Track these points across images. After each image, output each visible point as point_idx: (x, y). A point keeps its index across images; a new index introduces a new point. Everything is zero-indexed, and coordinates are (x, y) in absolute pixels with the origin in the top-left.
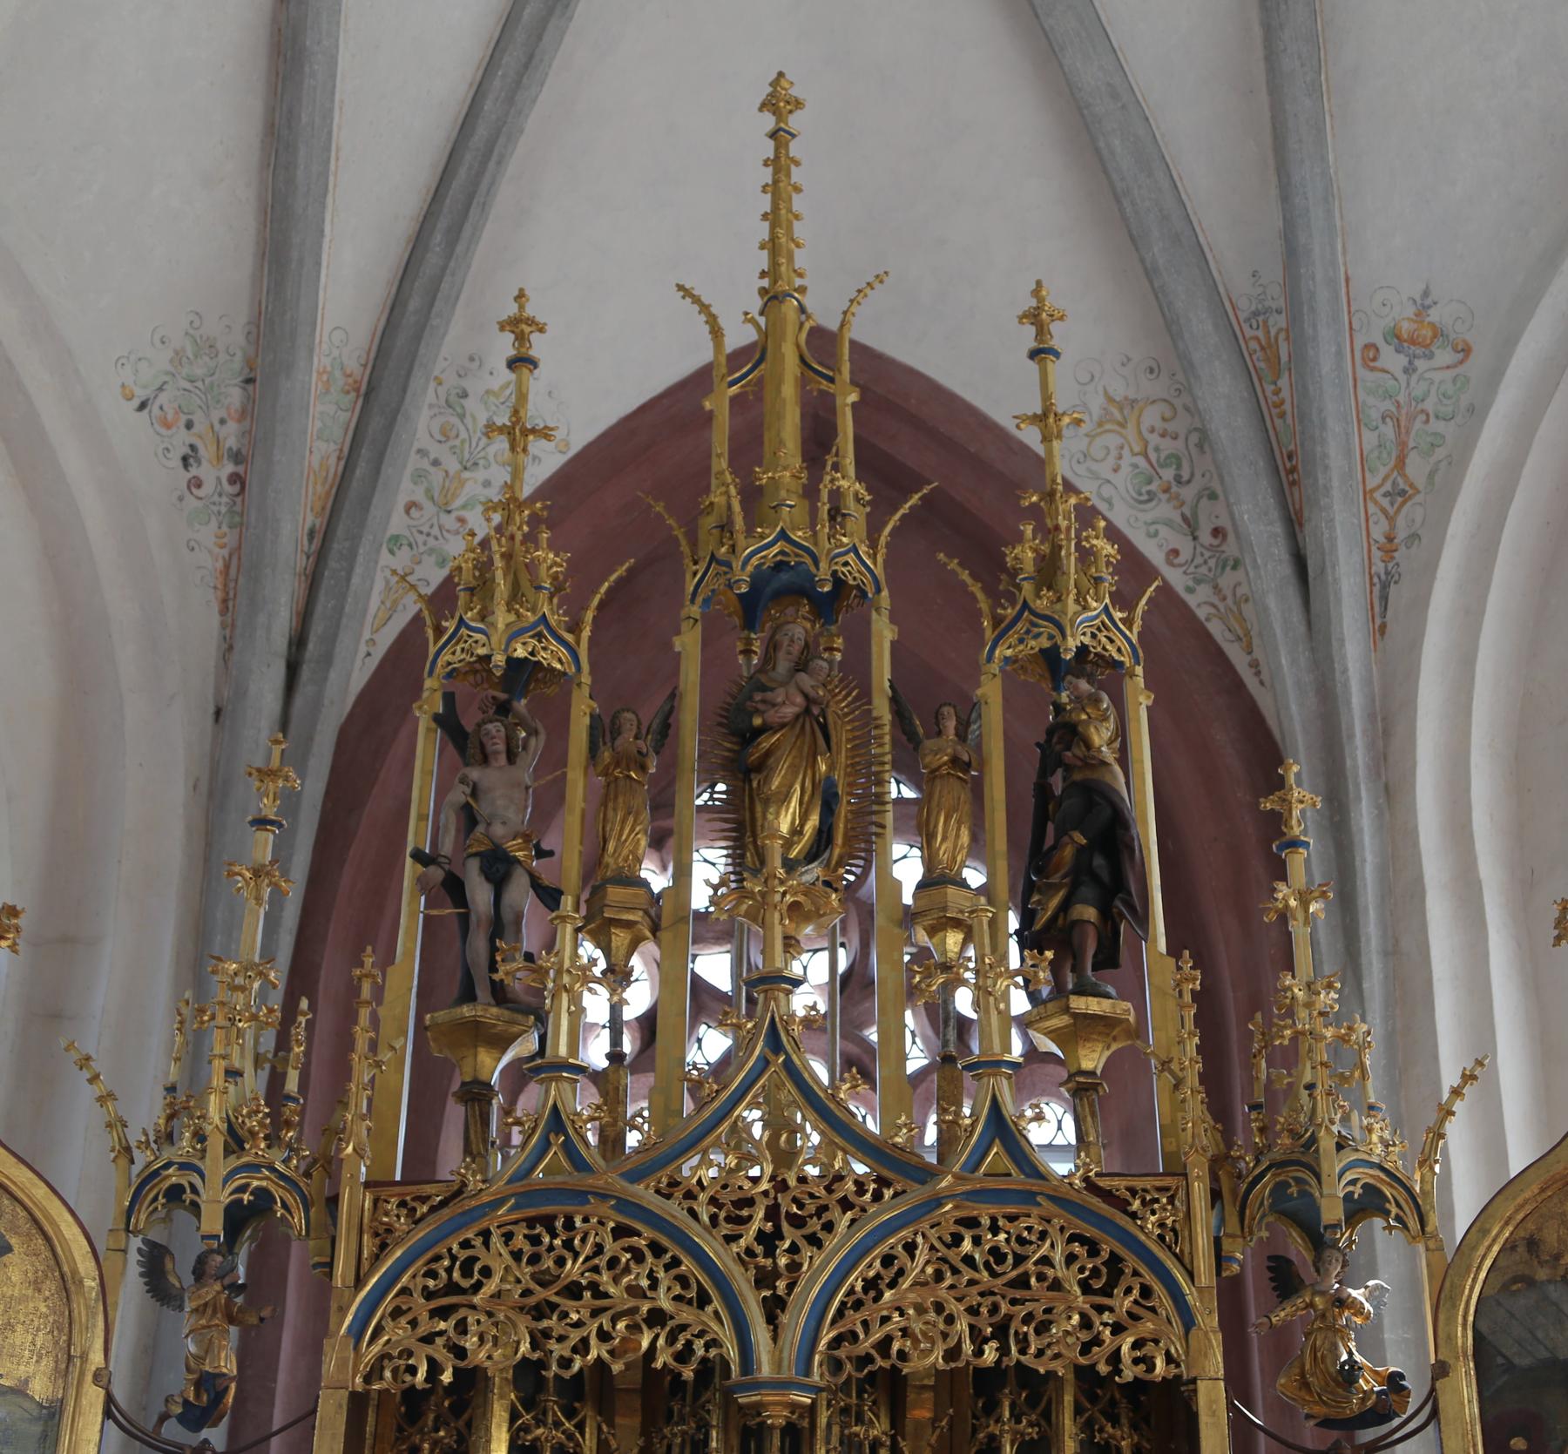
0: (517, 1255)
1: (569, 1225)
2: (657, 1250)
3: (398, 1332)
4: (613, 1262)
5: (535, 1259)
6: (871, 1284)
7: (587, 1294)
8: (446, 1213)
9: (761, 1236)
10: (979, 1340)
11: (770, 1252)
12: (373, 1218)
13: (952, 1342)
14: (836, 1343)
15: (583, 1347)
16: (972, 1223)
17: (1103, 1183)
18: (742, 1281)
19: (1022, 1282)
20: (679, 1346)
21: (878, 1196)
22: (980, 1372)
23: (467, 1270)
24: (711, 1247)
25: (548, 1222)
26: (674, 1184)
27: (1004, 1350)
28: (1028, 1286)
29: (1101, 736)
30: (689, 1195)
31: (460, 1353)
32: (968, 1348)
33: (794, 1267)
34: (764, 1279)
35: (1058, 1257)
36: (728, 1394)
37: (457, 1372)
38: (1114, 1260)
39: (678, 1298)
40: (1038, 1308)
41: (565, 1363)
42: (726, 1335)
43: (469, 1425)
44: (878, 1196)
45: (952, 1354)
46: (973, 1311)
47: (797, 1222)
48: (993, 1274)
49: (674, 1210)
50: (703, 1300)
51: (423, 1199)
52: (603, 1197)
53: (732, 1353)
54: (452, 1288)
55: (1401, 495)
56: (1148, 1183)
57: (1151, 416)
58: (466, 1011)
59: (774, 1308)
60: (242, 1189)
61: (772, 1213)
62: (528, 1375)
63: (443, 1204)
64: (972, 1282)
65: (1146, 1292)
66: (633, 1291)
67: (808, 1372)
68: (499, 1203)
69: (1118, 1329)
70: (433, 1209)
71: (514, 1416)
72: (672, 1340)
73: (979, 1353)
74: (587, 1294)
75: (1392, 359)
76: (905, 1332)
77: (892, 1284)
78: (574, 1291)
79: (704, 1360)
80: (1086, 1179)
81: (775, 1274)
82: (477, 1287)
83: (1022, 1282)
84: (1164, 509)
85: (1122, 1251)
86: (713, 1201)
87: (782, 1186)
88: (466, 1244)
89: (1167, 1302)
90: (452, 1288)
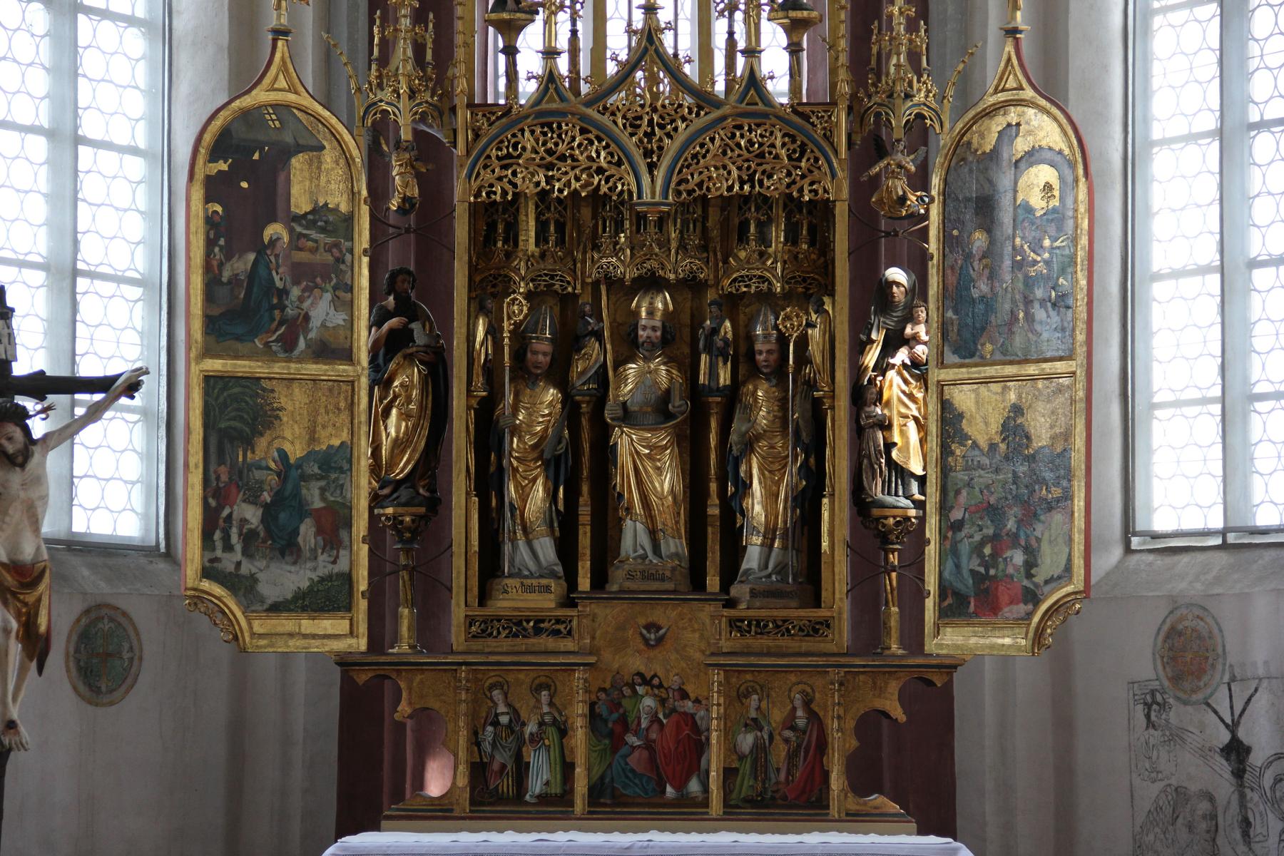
0: (537, 141)
1: (560, 127)
2: (600, 140)
3: (487, 176)
4: (580, 145)
5: (544, 144)
6: (695, 156)
7: (569, 161)
8: (504, 120)
9: (646, 134)
10: (742, 183)
11: (650, 142)
12: (472, 122)
13: (730, 182)
14: (679, 183)
15: (568, 184)
16: (740, 127)
17: (800, 109)
18: (637, 155)
19: (761, 155)
20: (610, 184)
21: (698, 115)
22: (741, 196)
23: (515, 148)
24: (624, 137)
25: (550, 125)
26: (605, 108)
27: (753, 187)
28: (764, 157)
30: (613, 114)
31: (515, 186)
32: (737, 188)
33: (660, 148)
34: (648, 153)
35: (778, 143)
36: (632, 206)
37: (514, 194)
38: (803, 145)
39: (610, 162)
40: (768, 167)
41: (561, 191)
42: (632, 179)
43: (518, 210)
44: (698, 115)
45: (730, 188)
46: (739, 168)
47: (662, 127)
48: (749, 151)
49: (606, 120)
50: (619, 163)
51: (493, 114)
52: (573, 114)
53: (635, 189)
54: (509, 156)
56: (820, 108)
58: (505, 16)
59: (651, 167)
60: (416, 113)
61: (651, 122)
62: (543, 195)
63: (502, 116)
64: (739, 156)
65: (817, 160)
66: (590, 158)
67: (667, 198)
68: (527, 117)
69: (803, 177)
70: (498, 118)
71: (537, 206)
72: (607, 182)
73: (741, 188)
74: (569, 161)
76: (710, 178)
77: (704, 157)
78: (562, 158)
79: (622, 191)
80: (792, 106)
81: (652, 152)
82: (519, 156)
83: (761, 155)
85: (806, 141)
86: (624, 117)
87: (655, 110)
88: (514, 135)
89: (826, 165)
90: (509, 156)
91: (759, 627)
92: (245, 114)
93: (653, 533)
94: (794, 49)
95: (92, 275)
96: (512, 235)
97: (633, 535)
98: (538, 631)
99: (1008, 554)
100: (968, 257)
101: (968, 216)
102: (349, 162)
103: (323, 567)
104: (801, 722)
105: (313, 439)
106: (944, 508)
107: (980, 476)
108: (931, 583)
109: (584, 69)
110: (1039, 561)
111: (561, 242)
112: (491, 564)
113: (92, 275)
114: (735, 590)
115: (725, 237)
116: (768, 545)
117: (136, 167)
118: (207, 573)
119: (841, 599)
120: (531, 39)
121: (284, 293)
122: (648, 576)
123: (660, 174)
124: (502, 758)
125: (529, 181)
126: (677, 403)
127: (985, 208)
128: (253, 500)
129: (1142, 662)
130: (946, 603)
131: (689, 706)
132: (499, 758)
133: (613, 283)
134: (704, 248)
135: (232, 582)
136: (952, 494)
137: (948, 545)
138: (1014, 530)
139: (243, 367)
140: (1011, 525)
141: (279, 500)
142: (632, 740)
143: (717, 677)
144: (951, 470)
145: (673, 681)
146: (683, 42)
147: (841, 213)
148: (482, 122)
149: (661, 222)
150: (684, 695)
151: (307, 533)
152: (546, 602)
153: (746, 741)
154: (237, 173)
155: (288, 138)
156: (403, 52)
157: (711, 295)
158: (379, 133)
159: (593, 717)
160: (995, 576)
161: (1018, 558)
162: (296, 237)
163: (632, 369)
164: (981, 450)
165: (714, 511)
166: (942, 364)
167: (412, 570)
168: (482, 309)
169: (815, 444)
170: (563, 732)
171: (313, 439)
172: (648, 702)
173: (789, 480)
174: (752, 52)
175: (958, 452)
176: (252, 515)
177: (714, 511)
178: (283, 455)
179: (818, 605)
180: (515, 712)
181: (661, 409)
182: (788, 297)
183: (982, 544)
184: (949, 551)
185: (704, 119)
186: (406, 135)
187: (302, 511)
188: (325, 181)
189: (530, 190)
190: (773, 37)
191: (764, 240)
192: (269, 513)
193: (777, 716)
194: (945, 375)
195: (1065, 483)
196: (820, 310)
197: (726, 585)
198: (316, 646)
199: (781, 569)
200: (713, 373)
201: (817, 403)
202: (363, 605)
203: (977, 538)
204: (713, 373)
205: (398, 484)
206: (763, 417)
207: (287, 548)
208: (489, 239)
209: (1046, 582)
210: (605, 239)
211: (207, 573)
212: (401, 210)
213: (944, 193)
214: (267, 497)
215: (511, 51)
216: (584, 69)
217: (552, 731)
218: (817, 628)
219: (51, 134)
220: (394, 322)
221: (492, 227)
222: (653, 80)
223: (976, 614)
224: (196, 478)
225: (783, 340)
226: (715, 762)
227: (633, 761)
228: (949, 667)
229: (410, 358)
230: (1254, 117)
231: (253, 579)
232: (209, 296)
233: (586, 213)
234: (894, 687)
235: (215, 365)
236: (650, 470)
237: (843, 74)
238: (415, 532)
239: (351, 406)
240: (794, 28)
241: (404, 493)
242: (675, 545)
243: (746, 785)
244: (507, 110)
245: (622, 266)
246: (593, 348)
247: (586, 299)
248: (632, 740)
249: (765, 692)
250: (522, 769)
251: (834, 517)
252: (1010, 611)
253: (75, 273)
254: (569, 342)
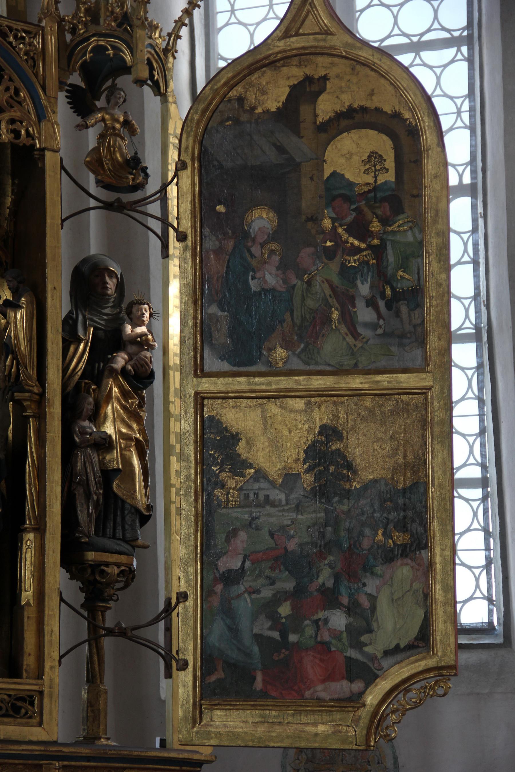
99: (321, 615)
107: (269, 515)
110: (375, 625)
119: (52, 668)
130: (213, 678)
136: (220, 539)
137: (216, 601)
138: (330, 584)
144: (219, 505)
160: (296, 645)
164: (272, 483)
175: (231, 483)
183: (276, 600)
195: (415, 526)
203: (267, 593)
209: (387, 653)
223: (264, 695)
252: (325, 690)
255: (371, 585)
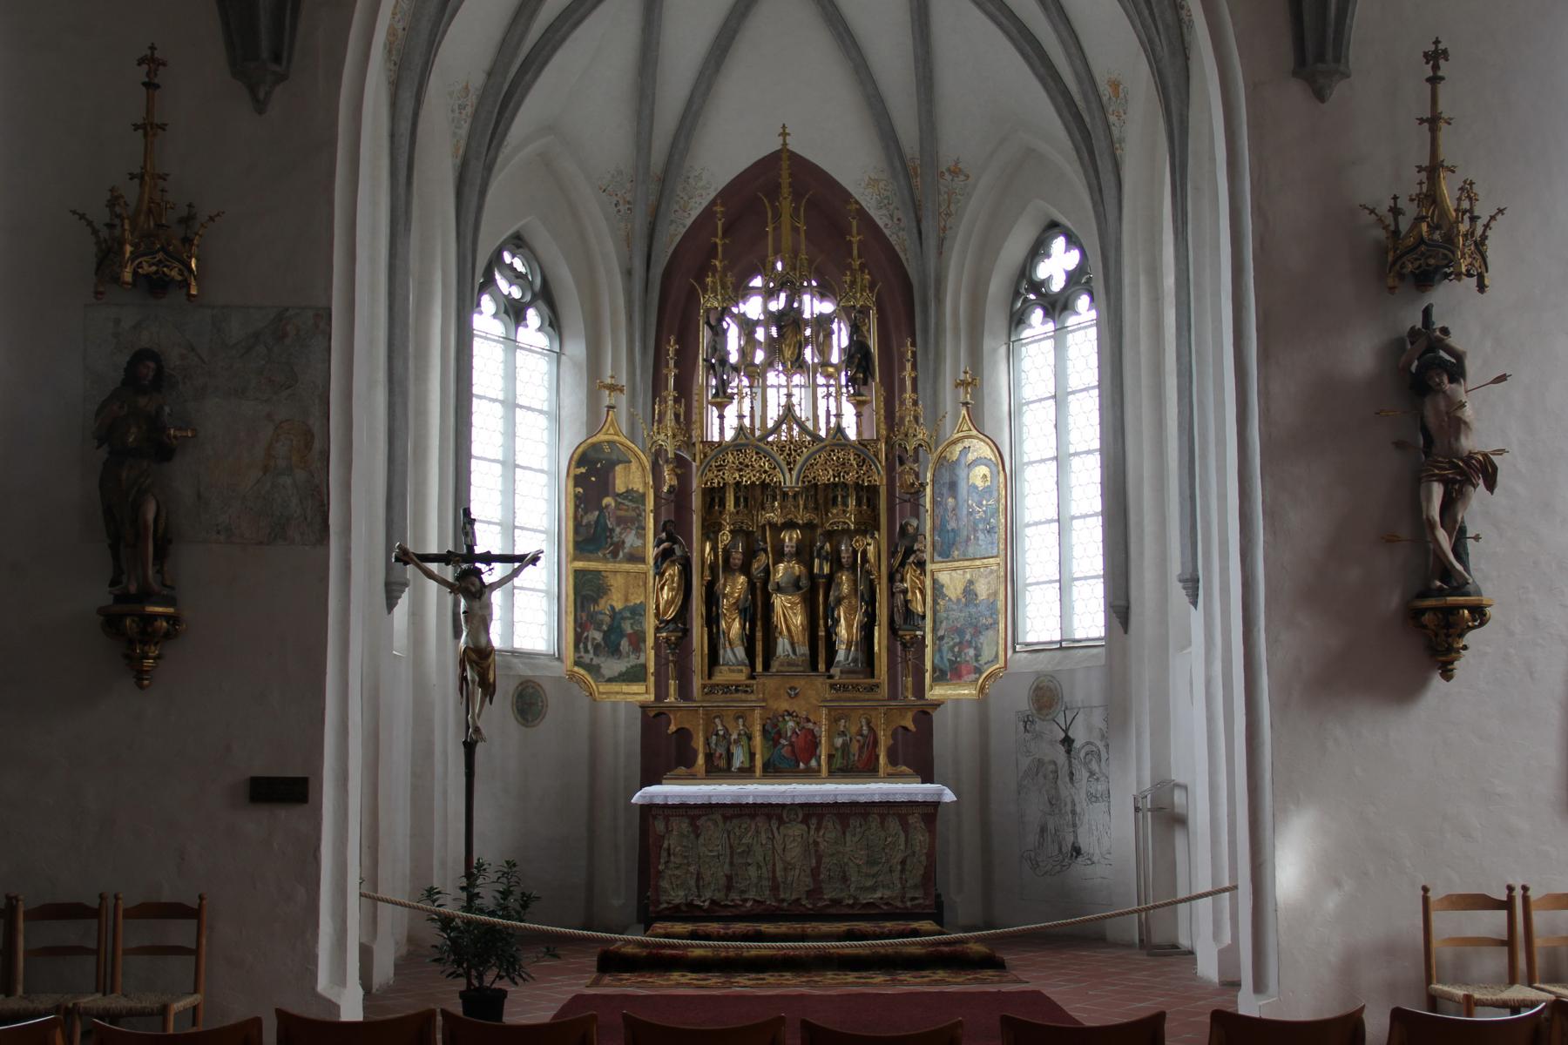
3: (710, 475)
18: (783, 464)
24: (777, 456)
29: (865, 329)
49: (768, 448)
55: (948, 215)
57: (881, 185)
59: (790, 470)
62: (738, 484)
75: (948, 176)
84: (884, 211)
91: (845, 687)
92: (594, 446)
93: (792, 644)
94: (859, 415)
95: (522, 528)
96: (722, 504)
97: (783, 645)
98: (737, 691)
100: (946, 510)
101: (945, 491)
102: (644, 469)
103: (632, 660)
104: (865, 732)
105: (627, 600)
106: (934, 630)
108: (928, 665)
109: (758, 424)
111: (746, 506)
112: (713, 659)
113: (522, 528)
114: (832, 671)
115: (826, 504)
116: (848, 649)
117: (543, 478)
118: (577, 663)
120: (731, 412)
121: (612, 530)
122: (790, 664)
123: (795, 473)
124: (721, 751)
125: (731, 477)
126: (804, 582)
127: (953, 486)
128: (598, 629)
129: (1024, 704)
131: (810, 725)
132: (719, 751)
133: (773, 526)
134: (816, 509)
135: (589, 668)
139: (593, 565)
140: (968, 637)
141: (611, 628)
142: (783, 742)
143: (824, 711)
145: (804, 714)
146: (802, 412)
147: (883, 491)
148: (708, 450)
149: (795, 496)
150: (808, 720)
151: (624, 644)
152: (741, 677)
153: (839, 742)
154: (590, 474)
155: (614, 457)
156: (670, 415)
157: (819, 531)
158: (657, 455)
159: (765, 732)
161: (971, 652)
162: (618, 504)
163: (781, 566)
165: (822, 633)
166: (933, 562)
167: (675, 663)
168: (708, 538)
169: (871, 601)
170: (750, 738)
171: (627, 600)
172: (791, 724)
173: (858, 618)
174: (839, 416)
176: (598, 636)
177: (822, 633)
178: (613, 608)
179: (872, 676)
180: (726, 730)
181: (796, 585)
182: (857, 532)
184: (938, 650)
185: (816, 447)
186: (670, 455)
187: (622, 634)
188: (632, 478)
189: (731, 481)
190: (849, 410)
191: (845, 504)
192: (606, 635)
193: (854, 729)
194: (935, 567)
196: (873, 537)
197: (828, 668)
198: (630, 699)
199: (855, 660)
200: (821, 568)
201: (872, 581)
202: (652, 679)
204: (821, 568)
205: (668, 622)
206: (845, 589)
207: (615, 651)
208: (711, 506)
210: (768, 505)
211: (577, 663)
212: (669, 492)
213: (933, 481)
214: (605, 628)
215: (721, 417)
216: (758, 424)
217: (744, 739)
218: (872, 688)
219: (503, 463)
220: (666, 545)
221: (713, 499)
222: (790, 429)
224: (571, 618)
225: (855, 552)
226: (823, 752)
227: (783, 751)
228: (937, 705)
229: (673, 563)
230: (1072, 451)
231: (598, 667)
232: (576, 532)
233: (758, 492)
234: (910, 715)
235: (580, 565)
236: (789, 613)
237: (883, 426)
238: (676, 645)
239: (645, 584)
240: (858, 405)
241: (671, 626)
242: (803, 649)
243: (838, 762)
244: (720, 443)
245: (774, 516)
246: (763, 557)
247: (758, 535)
248: (783, 742)
249: (847, 718)
250: (730, 756)
251: (880, 635)
253: (515, 527)
254: (750, 554)
255: (982, 639)
